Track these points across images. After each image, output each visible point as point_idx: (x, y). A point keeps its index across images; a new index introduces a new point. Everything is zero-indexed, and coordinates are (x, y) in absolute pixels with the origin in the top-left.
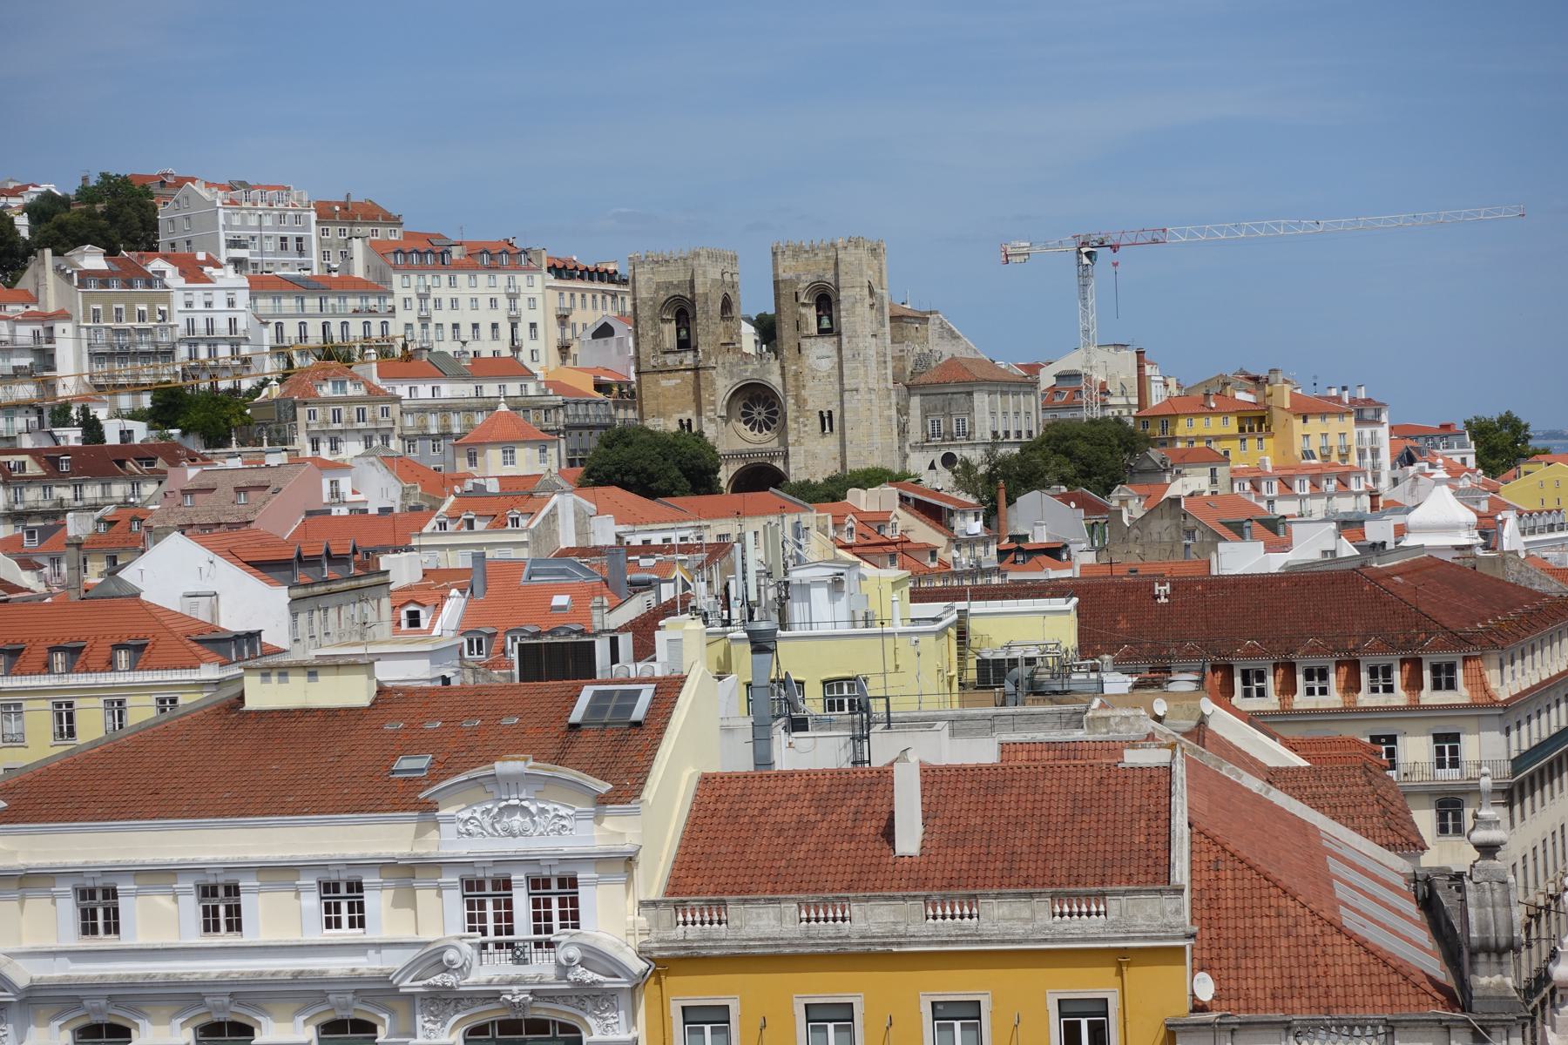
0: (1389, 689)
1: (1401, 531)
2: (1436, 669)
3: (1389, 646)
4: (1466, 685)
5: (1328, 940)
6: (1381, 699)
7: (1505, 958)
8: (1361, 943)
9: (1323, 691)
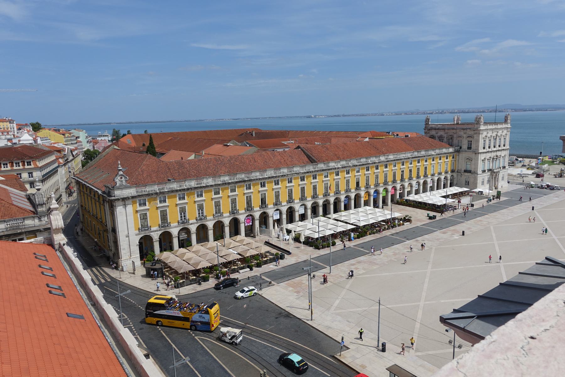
0: (19, 166)
1: (19, 141)
2: (27, 162)
3: (19, 159)
4: (33, 165)
5: (11, 207)
6: (18, 168)
7: (43, 206)
8: (17, 206)
9: (7, 167)
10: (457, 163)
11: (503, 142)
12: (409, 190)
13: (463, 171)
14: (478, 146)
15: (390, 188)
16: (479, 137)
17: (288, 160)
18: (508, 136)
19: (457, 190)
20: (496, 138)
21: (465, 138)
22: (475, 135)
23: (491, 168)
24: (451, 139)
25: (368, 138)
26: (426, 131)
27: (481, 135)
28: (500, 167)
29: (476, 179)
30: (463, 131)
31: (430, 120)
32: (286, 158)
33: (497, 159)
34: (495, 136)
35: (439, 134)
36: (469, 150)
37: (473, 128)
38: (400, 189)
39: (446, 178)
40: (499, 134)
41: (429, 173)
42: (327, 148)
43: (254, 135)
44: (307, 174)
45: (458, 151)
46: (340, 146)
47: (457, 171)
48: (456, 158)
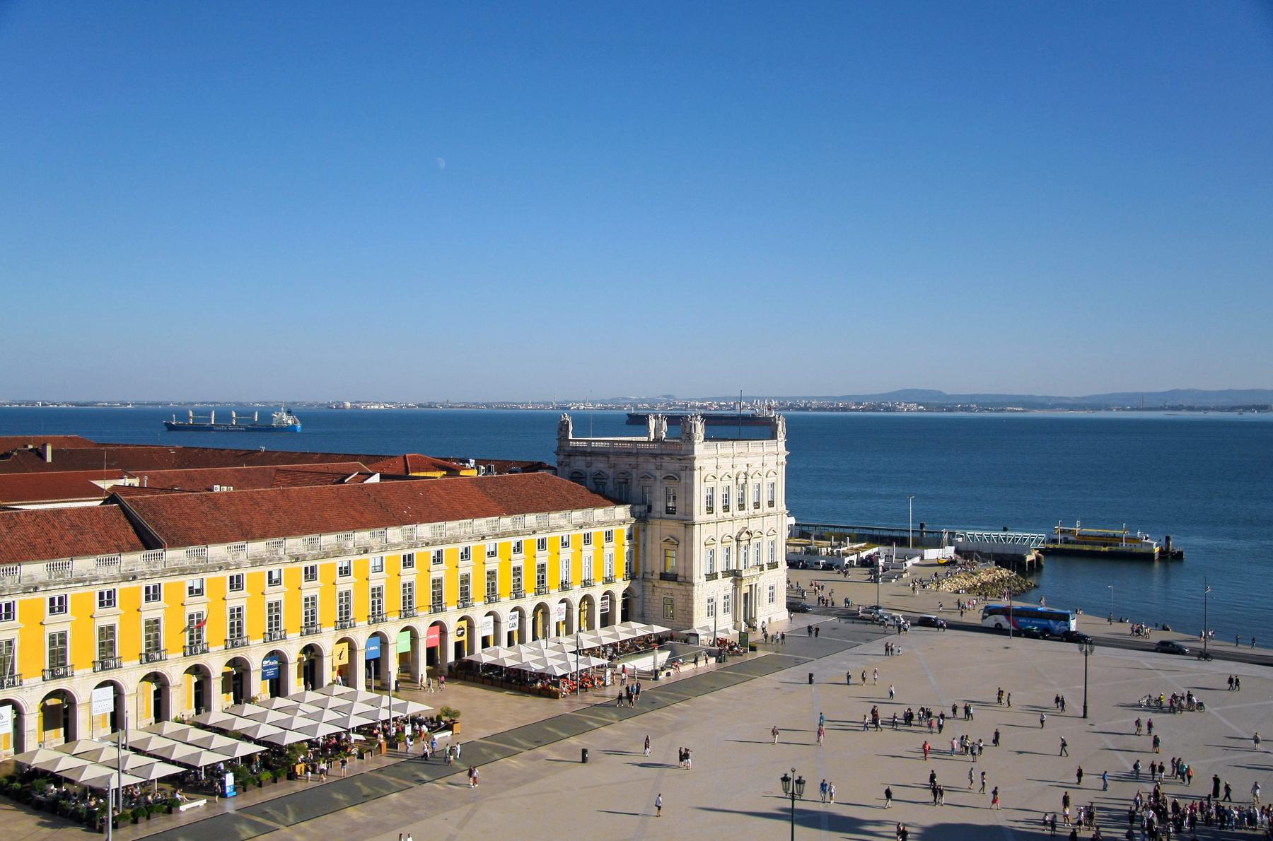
10: (641, 549)
11: (765, 495)
12: (489, 632)
13: (658, 577)
14: (690, 505)
15: (422, 624)
16: (692, 477)
17: (62, 538)
18: (779, 476)
19: (634, 631)
20: (746, 482)
21: (658, 483)
22: (683, 474)
23: (735, 568)
24: (624, 482)
25: (378, 474)
26: (562, 457)
27: (697, 473)
28: (762, 566)
29: (689, 599)
30: (654, 460)
31: (571, 428)
32: (55, 534)
33: (750, 540)
34: (742, 476)
35: (594, 469)
36: (671, 515)
37: (676, 452)
38: (459, 629)
39: (609, 595)
40: (751, 472)
41: (551, 580)
42: (215, 504)
43: (49, 459)
44: (125, 585)
45: (643, 518)
46: (263, 498)
47: (641, 577)
48: (637, 540)
